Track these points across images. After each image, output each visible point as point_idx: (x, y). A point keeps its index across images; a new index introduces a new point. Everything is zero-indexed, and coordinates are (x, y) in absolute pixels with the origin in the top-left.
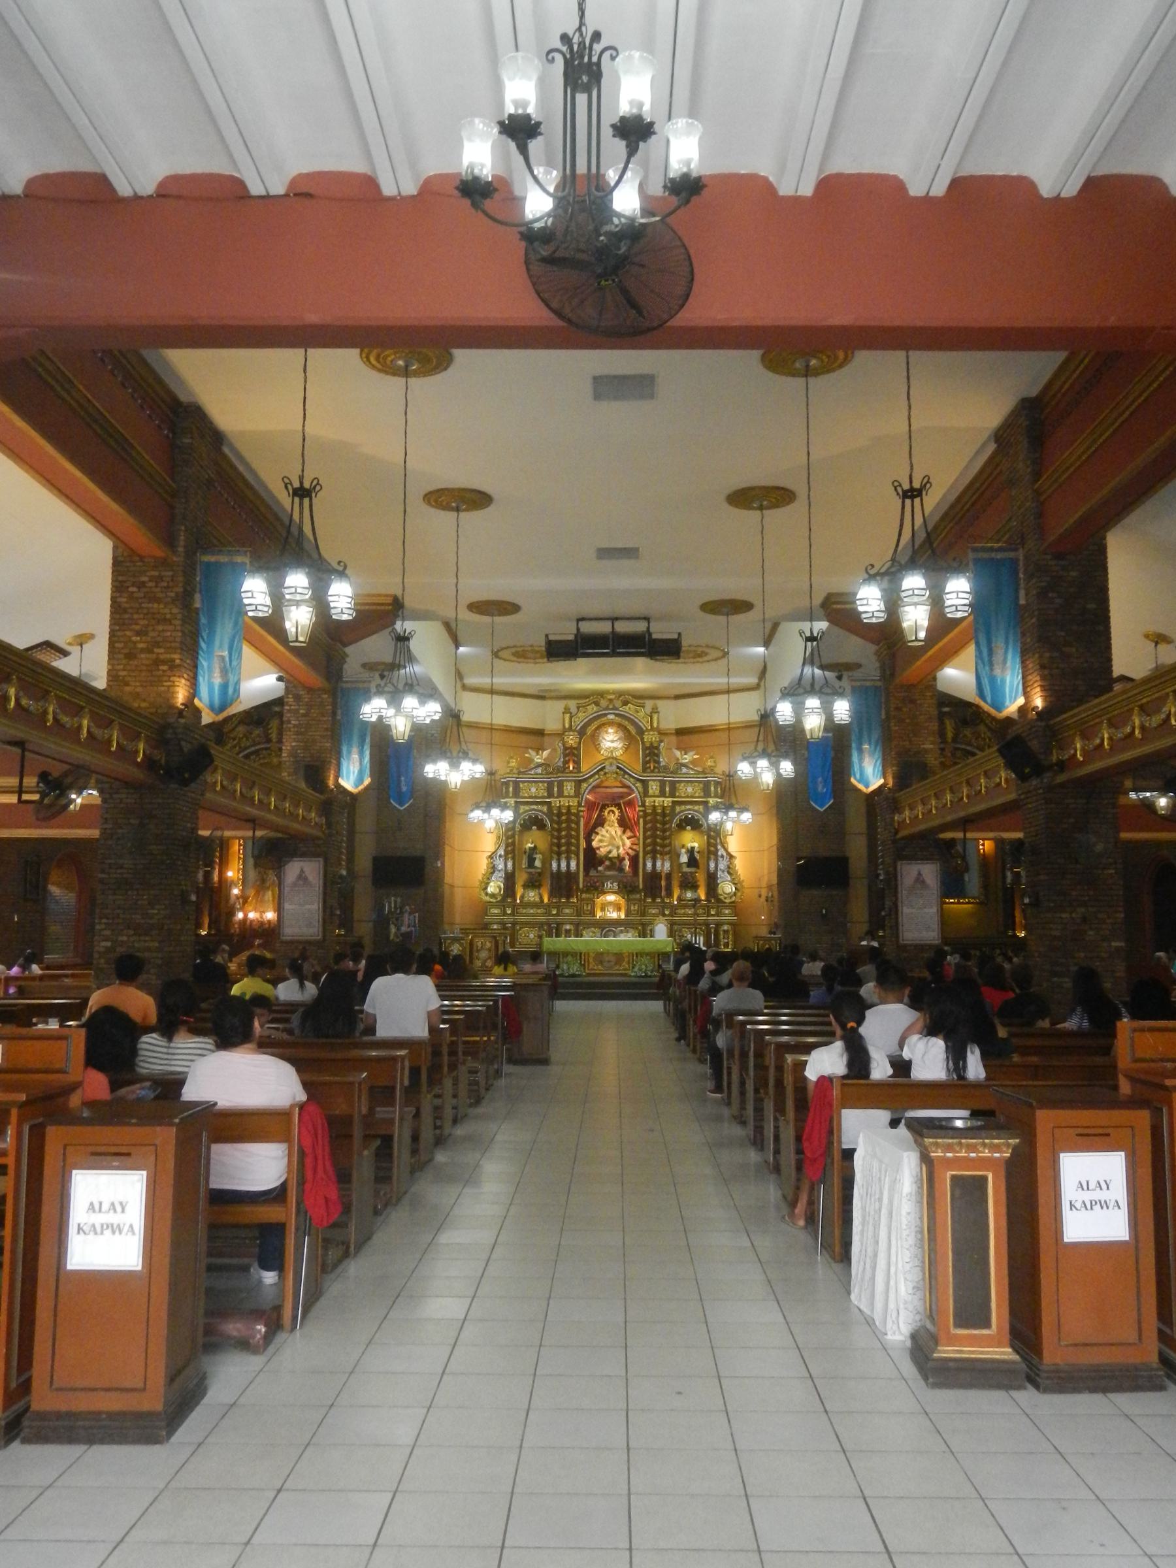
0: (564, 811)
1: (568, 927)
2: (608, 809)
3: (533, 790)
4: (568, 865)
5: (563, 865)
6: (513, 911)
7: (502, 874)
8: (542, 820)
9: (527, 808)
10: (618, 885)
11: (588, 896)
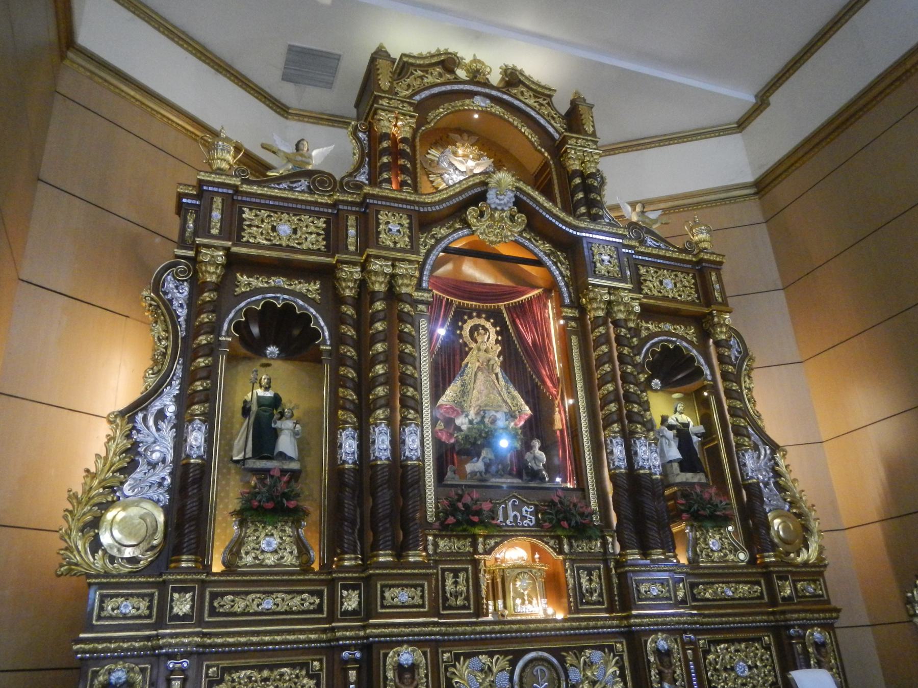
0: (379, 287)
1: (406, 656)
2: (470, 324)
3: (285, 229)
4: (397, 443)
5: (382, 443)
6: (198, 605)
7: (164, 473)
8: (306, 318)
9: (258, 282)
10: (535, 513)
11: (457, 545)
